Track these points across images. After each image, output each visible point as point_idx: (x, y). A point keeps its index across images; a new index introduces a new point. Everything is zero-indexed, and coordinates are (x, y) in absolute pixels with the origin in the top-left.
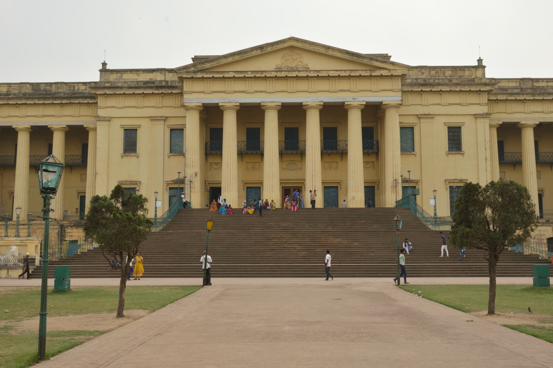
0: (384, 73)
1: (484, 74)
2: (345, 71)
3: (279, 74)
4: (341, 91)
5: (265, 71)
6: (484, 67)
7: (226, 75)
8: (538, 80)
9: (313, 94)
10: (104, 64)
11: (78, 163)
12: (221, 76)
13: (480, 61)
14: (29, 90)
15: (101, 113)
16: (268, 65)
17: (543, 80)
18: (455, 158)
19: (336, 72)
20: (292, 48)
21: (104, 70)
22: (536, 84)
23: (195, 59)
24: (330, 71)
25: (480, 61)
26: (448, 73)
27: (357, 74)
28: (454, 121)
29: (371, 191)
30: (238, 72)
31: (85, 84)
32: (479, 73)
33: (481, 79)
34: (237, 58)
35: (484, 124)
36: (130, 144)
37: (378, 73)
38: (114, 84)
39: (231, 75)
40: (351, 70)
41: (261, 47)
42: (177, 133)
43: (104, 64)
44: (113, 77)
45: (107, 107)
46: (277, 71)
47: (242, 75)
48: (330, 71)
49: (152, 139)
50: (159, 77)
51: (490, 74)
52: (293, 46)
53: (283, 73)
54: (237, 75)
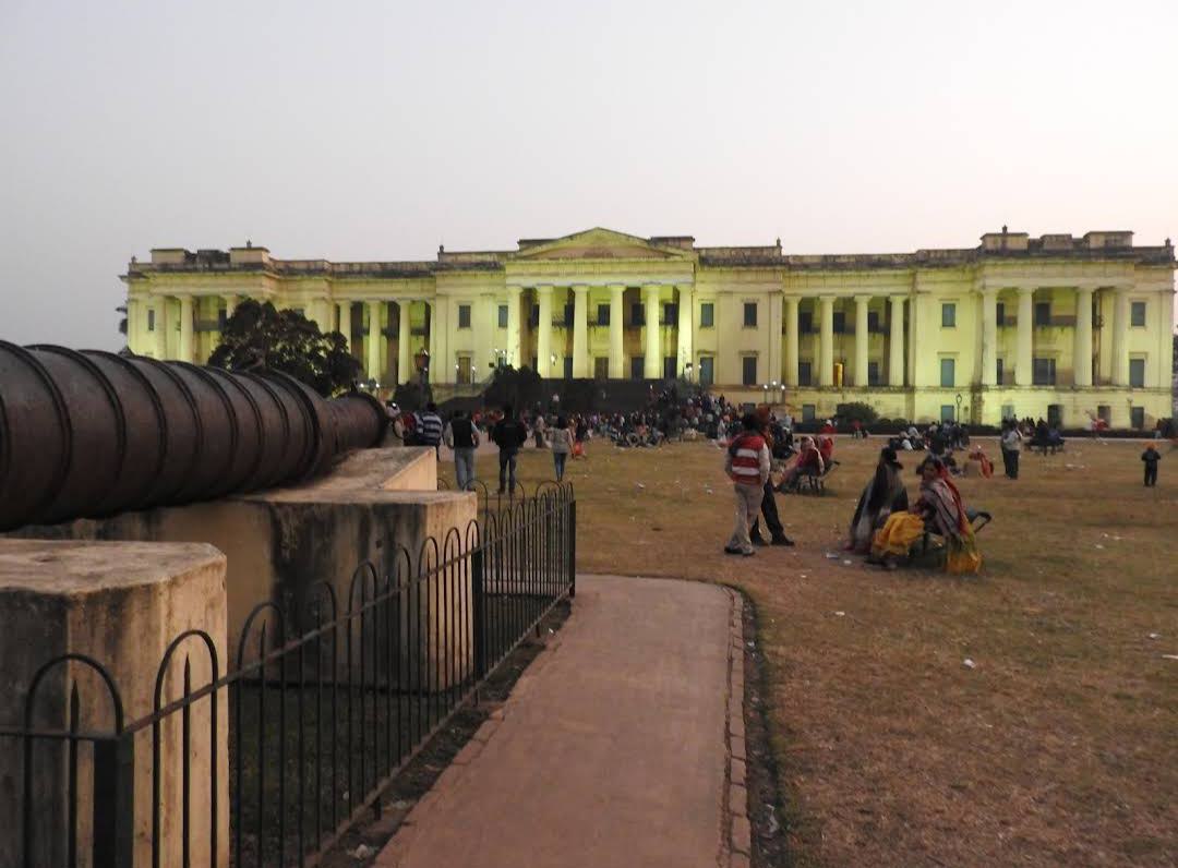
8: (839, 256)
10: (442, 248)
11: (423, 332)
13: (778, 241)
14: (378, 268)
15: (438, 291)
17: (844, 256)
18: (749, 331)
21: (441, 253)
22: (838, 260)
25: (778, 241)
26: (748, 253)
28: (751, 298)
29: (670, 363)
31: (427, 263)
33: (776, 259)
35: (777, 301)
36: (465, 318)
38: (449, 264)
42: (503, 310)
43: (442, 248)
44: (449, 259)
45: (445, 284)
49: (484, 314)
50: (489, 259)
51: (785, 252)
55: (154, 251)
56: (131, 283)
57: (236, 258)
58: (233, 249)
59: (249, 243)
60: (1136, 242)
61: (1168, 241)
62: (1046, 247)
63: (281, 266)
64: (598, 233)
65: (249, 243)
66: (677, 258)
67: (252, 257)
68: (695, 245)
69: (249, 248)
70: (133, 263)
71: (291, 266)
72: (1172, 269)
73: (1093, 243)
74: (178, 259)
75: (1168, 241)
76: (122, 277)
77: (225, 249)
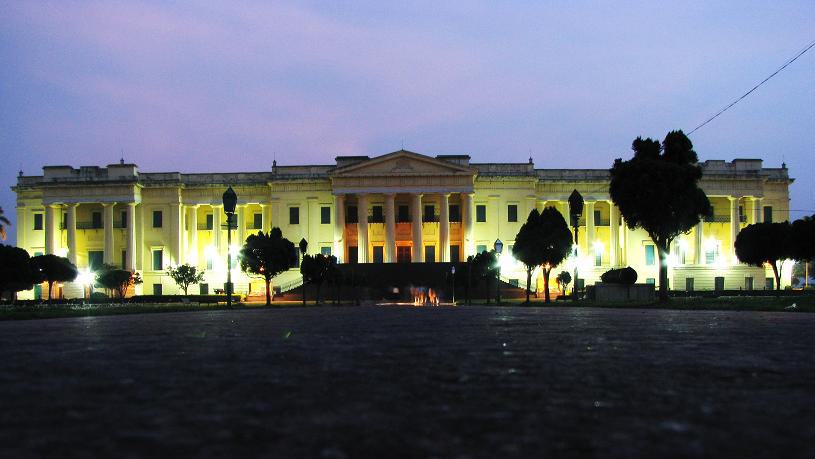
0: (463, 173)
7: (361, 175)
13: (531, 159)
16: (387, 168)
21: (274, 166)
23: (338, 159)
25: (531, 159)
27: (446, 173)
32: (529, 167)
44: (280, 172)
55: (45, 168)
56: (19, 192)
57: (113, 175)
58: (110, 166)
59: (122, 160)
60: (764, 165)
61: (784, 165)
62: (710, 168)
63: (144, 178)
64: (403, 154)
65: (122, 160)
66: (463, 173)
67: (125, 172)
68: (471, 161)
69: (123, 165)
70: (21, 177)
71: (151, 177)
72: (786, 184)
73: (740, 167)
74: (67, 174)
75: (784, 165)
76: (13, 188)
77: (103, 166)
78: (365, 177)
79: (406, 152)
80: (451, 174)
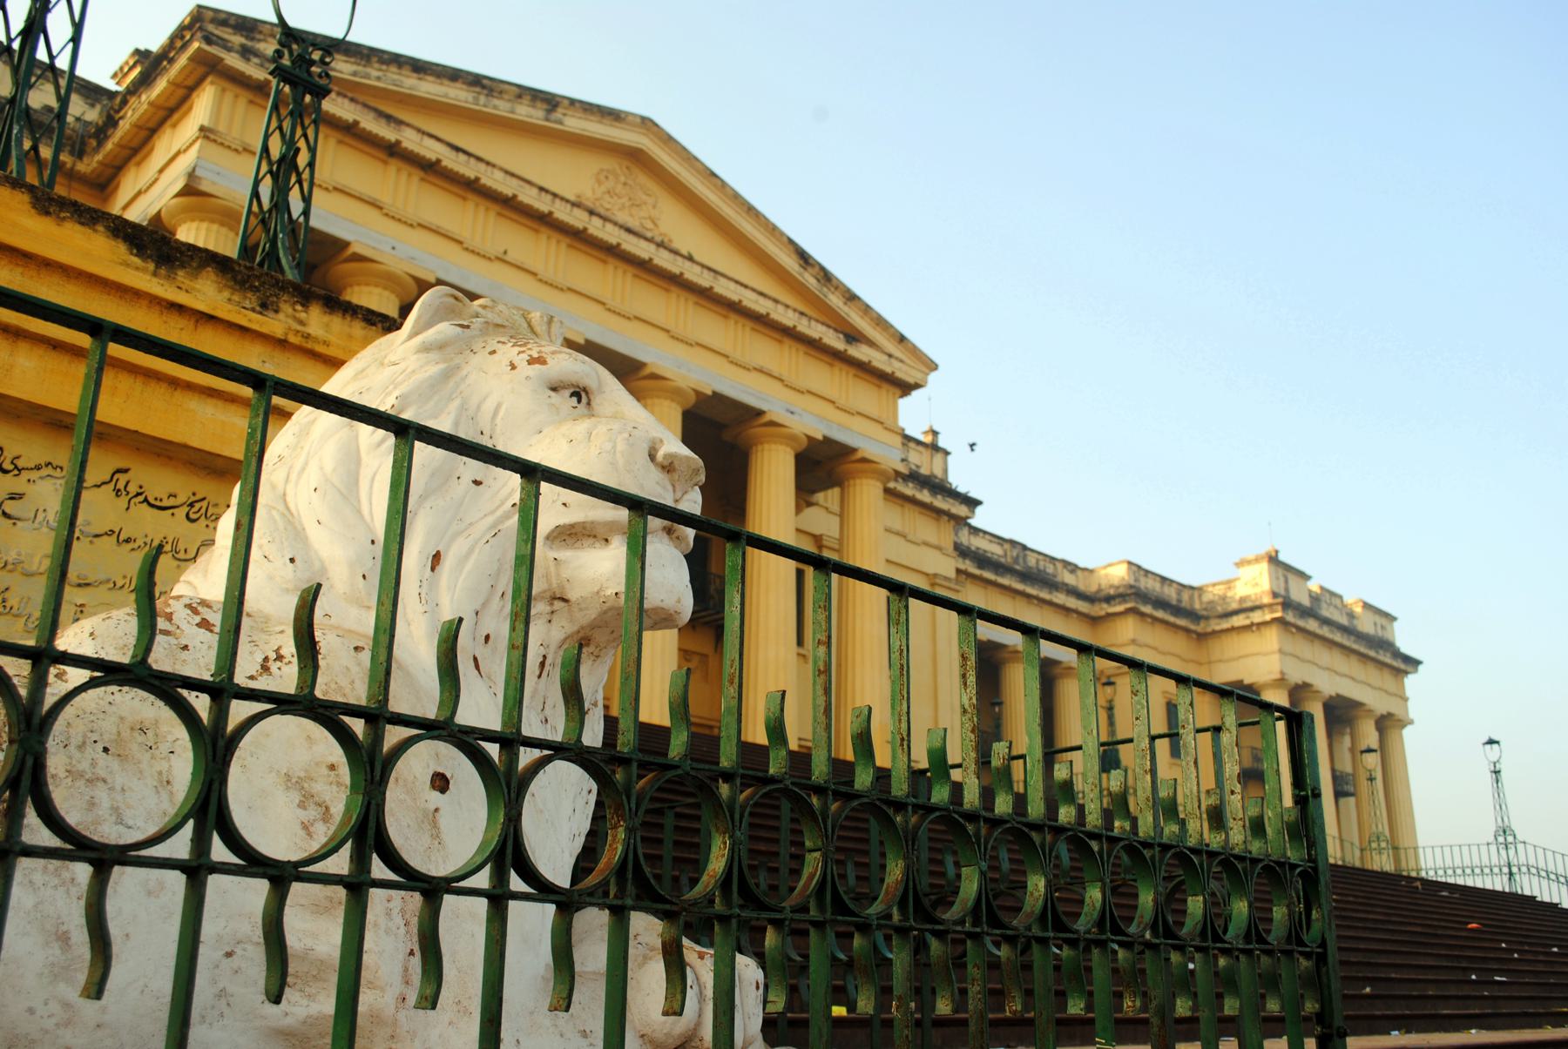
0: (879, 361)
1: (945, 471)
2: (787, 306)
3: (596, 228)
4: (761, 371)
5: (555, 195)
6: (947, 453)
7: (410, 140)
9: (681, 346)
12: (387, 133)
19: (761, 300)
20: (636, 157)
24: (746, 287)
30: (457, 149)
34: (458, 94)
37: (861, 352)
39: (430, 150)
40: (802, 314)
41: (550, 101)
46: (592, 213)
47: (468, 169)
48: (746, 287)
52: (639, 152)
53: (609, 227)
54: (451, 161)
78: (430, 168)
79: (668, 140)
80: (834, 341)
